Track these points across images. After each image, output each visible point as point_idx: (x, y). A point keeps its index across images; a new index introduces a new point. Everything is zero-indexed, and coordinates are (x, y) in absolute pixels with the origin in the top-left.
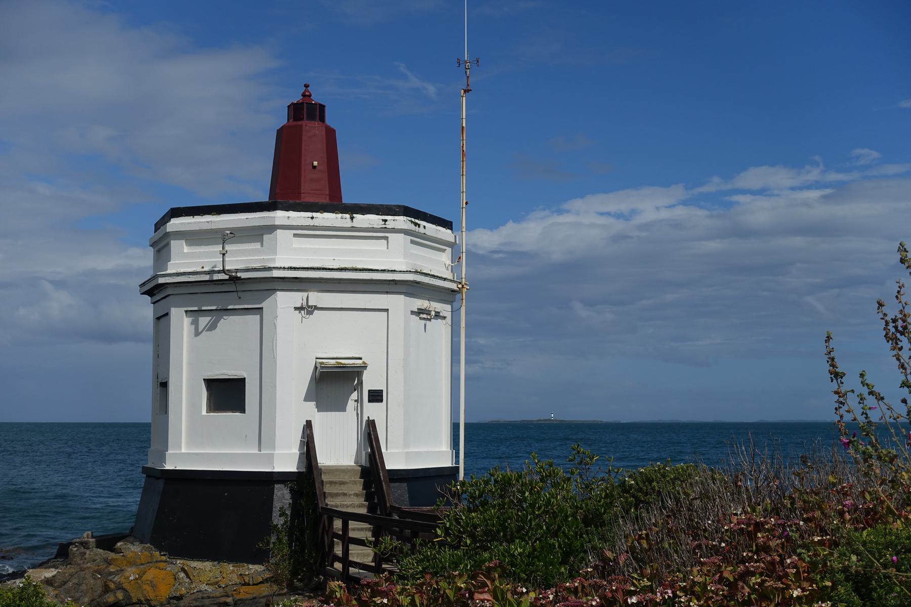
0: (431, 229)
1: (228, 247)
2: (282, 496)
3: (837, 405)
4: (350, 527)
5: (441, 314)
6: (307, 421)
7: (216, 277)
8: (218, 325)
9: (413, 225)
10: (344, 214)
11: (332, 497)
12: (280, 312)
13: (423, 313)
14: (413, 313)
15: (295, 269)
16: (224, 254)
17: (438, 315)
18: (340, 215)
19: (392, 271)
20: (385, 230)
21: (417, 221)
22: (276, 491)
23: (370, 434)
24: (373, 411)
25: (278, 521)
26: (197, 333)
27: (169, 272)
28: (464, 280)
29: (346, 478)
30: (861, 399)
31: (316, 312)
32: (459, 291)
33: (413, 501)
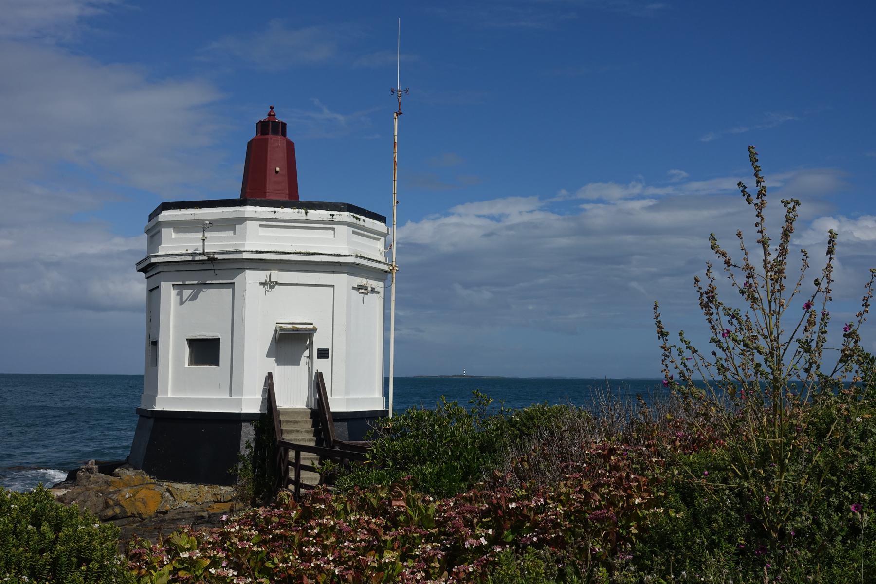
0: (369, 222)
1: (207, 234)
2: (248, 433)
3: (663, 358)
4: (301, 457)
5: (376, 290)
6: (268, 373)
7: (197, 258)
8: (199, 296)
9: (354, 219)
10: (300, 210)
11: (288, 433)
12: (248, 286)
13: (362, 289)
14: (353, 288)
15: (261, 252)
16: (204, 240)
17: (373, 291)
18: (297, 210)
19: (337, 255)
20: (332, 222)
21: (358, 216)
22: (243, 428)
23: (318, 384)
24: (321, 365)
25: (244, 452)
27: (160, 253)
28: (394, 263)
29: (299, 419)
30: (680, 352)
31: (277, 286)
32: (391, 272)
33: (352, 437)
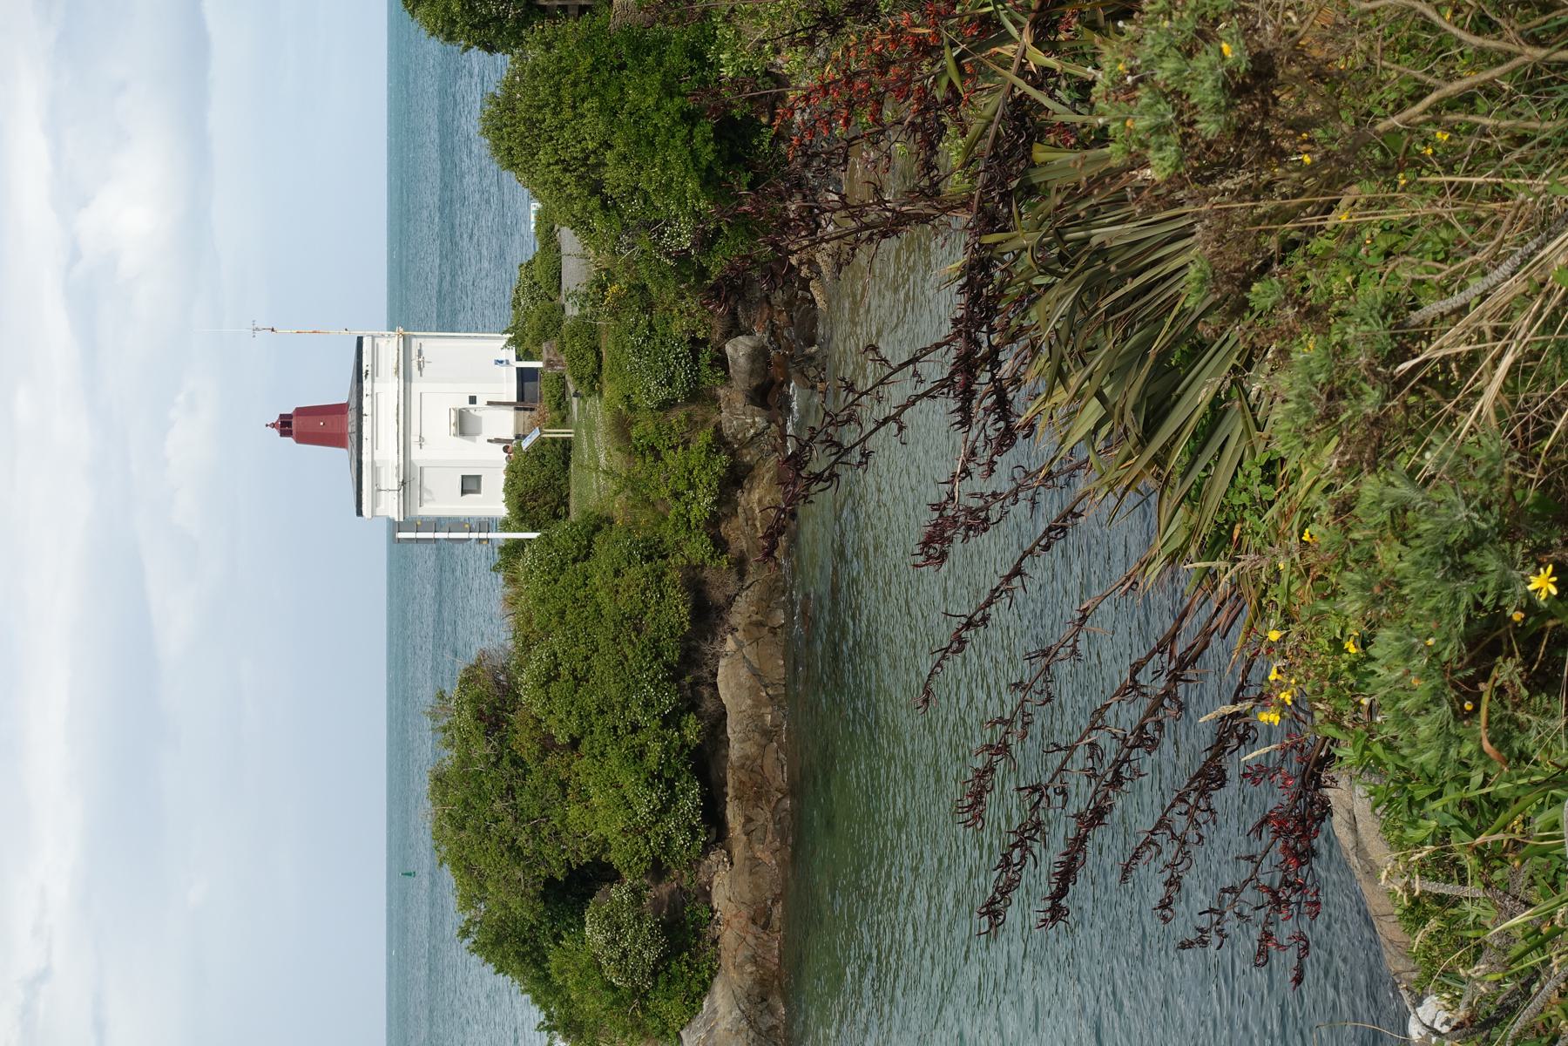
24: (481, 402)
26: (433, 500)
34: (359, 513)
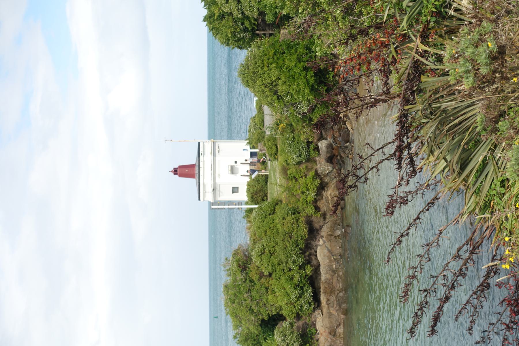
24: (238, 163)
34: (199, 199)
